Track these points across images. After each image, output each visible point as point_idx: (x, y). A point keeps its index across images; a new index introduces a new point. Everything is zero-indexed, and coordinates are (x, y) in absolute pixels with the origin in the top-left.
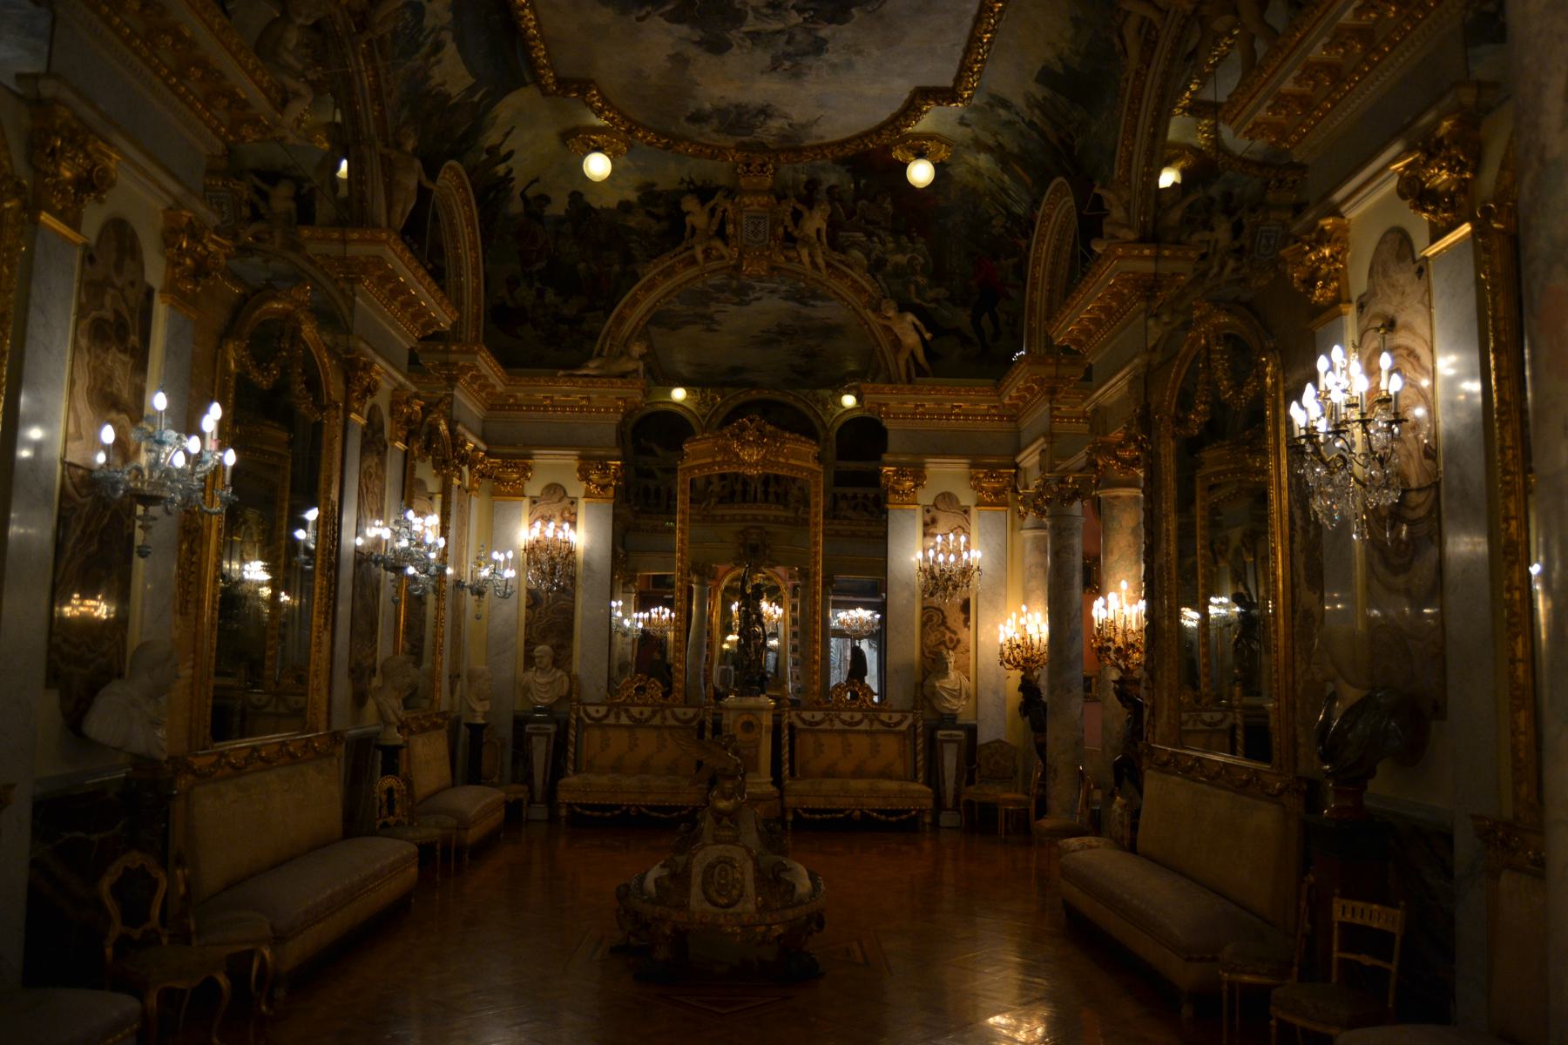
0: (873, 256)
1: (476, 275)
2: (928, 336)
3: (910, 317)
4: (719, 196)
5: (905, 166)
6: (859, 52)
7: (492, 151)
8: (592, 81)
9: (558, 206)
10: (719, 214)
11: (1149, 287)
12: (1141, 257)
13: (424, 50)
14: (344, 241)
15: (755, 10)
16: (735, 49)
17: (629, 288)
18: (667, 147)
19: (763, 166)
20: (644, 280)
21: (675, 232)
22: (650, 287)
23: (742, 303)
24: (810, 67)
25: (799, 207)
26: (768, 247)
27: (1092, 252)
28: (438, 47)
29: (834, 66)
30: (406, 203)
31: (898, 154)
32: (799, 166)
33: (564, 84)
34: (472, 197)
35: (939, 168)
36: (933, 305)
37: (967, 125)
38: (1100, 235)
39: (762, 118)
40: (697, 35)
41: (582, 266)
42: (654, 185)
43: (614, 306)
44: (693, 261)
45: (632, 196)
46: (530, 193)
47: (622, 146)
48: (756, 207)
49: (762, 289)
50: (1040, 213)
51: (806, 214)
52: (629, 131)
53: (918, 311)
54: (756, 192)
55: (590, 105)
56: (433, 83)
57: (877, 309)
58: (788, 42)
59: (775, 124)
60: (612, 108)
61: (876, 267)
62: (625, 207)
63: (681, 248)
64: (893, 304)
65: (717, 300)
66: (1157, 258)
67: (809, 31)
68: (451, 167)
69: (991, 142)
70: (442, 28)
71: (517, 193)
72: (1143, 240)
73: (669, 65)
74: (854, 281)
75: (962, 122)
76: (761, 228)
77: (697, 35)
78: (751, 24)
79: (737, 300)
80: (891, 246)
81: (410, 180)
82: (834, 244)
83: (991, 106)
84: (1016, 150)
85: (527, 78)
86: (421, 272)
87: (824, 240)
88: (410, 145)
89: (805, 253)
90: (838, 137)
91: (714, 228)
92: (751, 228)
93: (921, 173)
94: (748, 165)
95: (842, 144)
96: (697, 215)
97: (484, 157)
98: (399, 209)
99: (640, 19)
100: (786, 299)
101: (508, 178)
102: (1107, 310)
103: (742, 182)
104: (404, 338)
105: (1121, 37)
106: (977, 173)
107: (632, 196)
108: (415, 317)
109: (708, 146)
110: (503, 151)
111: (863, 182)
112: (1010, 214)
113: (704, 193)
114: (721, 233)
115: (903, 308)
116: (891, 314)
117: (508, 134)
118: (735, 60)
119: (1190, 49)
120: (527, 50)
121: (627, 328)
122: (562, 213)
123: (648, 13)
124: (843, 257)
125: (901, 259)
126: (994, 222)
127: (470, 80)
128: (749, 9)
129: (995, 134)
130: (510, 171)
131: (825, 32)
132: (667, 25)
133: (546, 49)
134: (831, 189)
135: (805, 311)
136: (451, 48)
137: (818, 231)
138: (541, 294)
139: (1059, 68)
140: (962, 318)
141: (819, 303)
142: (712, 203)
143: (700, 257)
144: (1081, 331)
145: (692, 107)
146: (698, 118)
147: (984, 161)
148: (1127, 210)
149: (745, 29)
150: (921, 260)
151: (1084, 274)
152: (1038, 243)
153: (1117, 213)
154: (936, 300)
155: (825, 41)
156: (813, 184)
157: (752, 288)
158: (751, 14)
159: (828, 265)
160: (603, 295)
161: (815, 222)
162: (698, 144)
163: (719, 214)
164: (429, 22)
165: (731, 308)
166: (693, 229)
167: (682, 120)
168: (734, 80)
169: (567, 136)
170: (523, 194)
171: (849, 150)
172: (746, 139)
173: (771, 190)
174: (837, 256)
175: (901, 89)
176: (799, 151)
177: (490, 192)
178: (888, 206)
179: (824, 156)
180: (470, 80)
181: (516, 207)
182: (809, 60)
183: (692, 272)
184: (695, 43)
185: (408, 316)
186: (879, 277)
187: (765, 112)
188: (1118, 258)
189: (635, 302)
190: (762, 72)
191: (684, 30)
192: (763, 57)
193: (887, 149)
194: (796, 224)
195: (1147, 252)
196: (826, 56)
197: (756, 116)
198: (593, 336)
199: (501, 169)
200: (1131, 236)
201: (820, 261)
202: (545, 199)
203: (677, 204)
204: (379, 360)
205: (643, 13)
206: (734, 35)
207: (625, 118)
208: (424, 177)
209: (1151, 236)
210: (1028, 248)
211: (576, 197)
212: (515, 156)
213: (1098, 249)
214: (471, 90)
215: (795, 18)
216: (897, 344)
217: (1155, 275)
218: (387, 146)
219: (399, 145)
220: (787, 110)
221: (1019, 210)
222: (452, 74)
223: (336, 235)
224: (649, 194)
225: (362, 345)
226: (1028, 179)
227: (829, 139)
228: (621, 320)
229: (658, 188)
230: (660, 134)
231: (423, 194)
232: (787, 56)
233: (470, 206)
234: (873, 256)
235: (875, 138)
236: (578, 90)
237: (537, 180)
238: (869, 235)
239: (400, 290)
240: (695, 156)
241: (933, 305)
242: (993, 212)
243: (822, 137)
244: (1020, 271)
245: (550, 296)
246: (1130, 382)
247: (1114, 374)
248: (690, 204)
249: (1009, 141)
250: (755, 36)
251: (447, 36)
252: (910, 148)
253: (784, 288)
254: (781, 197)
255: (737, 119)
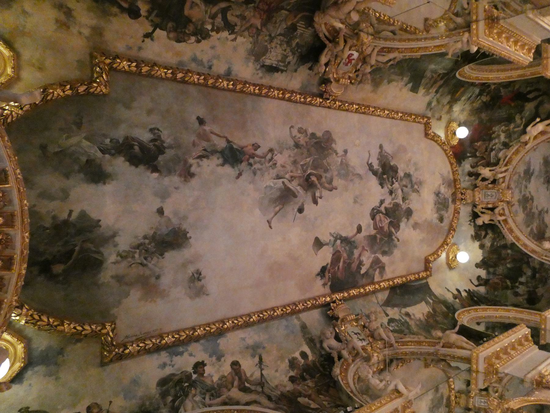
0: (502, 147)
1: (509, 311)
2: (538, 120)
3: (529, 128)
4: (476, 210)
5: (460, 140)
6: (410, 161)
7: (455, 297)
8: (425, 258)
9: (483, 273)
10: (484, 210)
11: (492, 21)
12: (477, 29)
13: (408, 319)
14: (477, 372)
15: (393, 199)
16: (411, 206)
17: (518, 247)
18: (454, 230)
19: (462, 194)
20: (514, 241)
21: (491, 227)
22: (518, 239)
23: (532, 199)
24: (417, 178)
25: (480, 178)
26: (498, 190)
27: (478, 51)
28: (407, 314)
29: (416, 170)
30: (462, 340)
31: (455, 142)
32: (462, 180)
33: (427, 268)
34: (473, 308)
35: (460, 125)
36: (524, 120)
37: (441, 117)
38: (469, 51)
39: (440, 195)
40: (404, 220)
41: (509, 266)
42: (472, 236)
43: (526, 254)
44: (505, 221)
45: (477, 244)
46: (476, 283)
47: (455, 247)
48: (480, 196)
49: (525, 191)
50: (477, 82)
51: (483, 176)
52: (447, 245)
53: (526, 125)
54: (474, 196)
55: (435, 259)
56: (422, 318)
57: (526, 143)
58: (406, 187)
59: (443, 190)
60: (437, 251)
61: (506, 146)
62: (482, 247)
63: (499, 225)
64: (523, 136)
65: (531, 209)
66: (477, 21)
67: (401, 180)
68: (459, 315)
69: (448, 107)
70: (400, 312)
71: (476, 289)
72: (469, 31)
73: (418, 230)
74: (513, 153)
75: (440, 119)
76: (489, 193)
77: (404, 220)
78: (399, 201)
79: (531, 202)
80: (497, 141)
81: (453, 337)
82: (496, 164)
83: (431, 109)
84: (450, 96)
85: (424, 281)
86: (496, 339)
87: (494, 168)
88: (439, 334)
89: (500, 176)
90: (449, 166)
91: (490, 212)
92: (489, 197)
93: (463, 133)
94: (462, 199)
95: (451, 164)
96: (485, 219)
97: (457, 300)
98: (465, 345)
99: (398, 240)
100: (530, 182)
101: (469, 292)
102: (508, 39)
103: (469, 201)
104: (535, 351)
105: (390, 60)
106: (463, 110)
107: (477, 244)
108: (521, 344)
109: (454, 215)
110: (456, 292)
111: (468, 155)
112: (480, 94)
113: (475, 216)
114: (492, 209)
115: (524, 132)
116: (527, 138)
117: (448, 290)
118: (414, 205)
119: (391, 34)
120: (411, 281)
121: (537, 249)
122: (485, 271)
123: (396, 237)
124: (502, 160)
125: (503, 137)
126: (485, 100)
127: (423, 303)
128: (393, 202)
129: (443, 106)
130: (465, 290)
131: (401, 174)
132: (400, 231)
133: (411, 274)
134: (472, 167)
135: (536, 173)
136: (409, 310)
137: (490, 171)
138: (521, 283)
139: (410, 85)
140: (530, 107)
141: (532, 168)
142: (480, 214)
143: (503, 218)
144: (523, 49)
145: (436, 221)
146: (441, 219)
147: (457, 108)
148: (458, 41)
149: (401, 203)
150: (503, 127)
151: (493, 54)
152: (489, 80)
153: (459, 45)
154: (521, 119)
155: (405, 174)
156: (470, 174)
157: (524, 196)
158: (395, 201)
159: (506, 165)
160: (522, 258)
161: (486, 172)
162: (453, 219)
163: (484, 210)
164: (397, 317)
165: (535, 203)
166: (491, 220)
167: (442, 225)
168: (424, 206)
169: (450, 268)
170: (476, 286)
171: (453, 161)
172: (450, 200)
173: (473, 190)
174: (501, 162)
175: (426, 143)
176: (455, 181)
177: (473, 299)
178: (479, 144)
179: (456, 170)
180: (423, 303)
181: (482, 290)
182: (414, 179)
183: (510, 221)
184: (408, 220)
185: (519, 348)
186: (511, 144)
187: (438, 194)
188: (478, 38)
189: (525, 245)
190: (420, 196)
191: (402, 225)
192: (413, 196)
193: (453, 147)
194: (487, 180)
195: (474, 27)
196: (412, 173)
197: (439, 197)
198: (542, 264)
199: (464, 294)
200: (467, 35)
201: (504, 169)
202: (479, 278)
203: (480, 227)
204: (540, 368)
205: (396, 239)
206: (404, 206)
207: (442, 246)
208: (453, 331)
209: (468, 27)
210: (495, 84)
211: (477, 266)
212: (458, 288)
213: (475, 49)
214: (427, 303)
215: (396, 185)
216: (542, 133)
217: (485, 19)
218: (440, 343)
219: (440, 338)
220: (436, 185)
221: (477, 91)
222: (420, 311)
223: (474, 374)
224: (477, 237)
225: (530, 376)
226: (462, 89)
227: (450, 170)
228: (533, 251)
229: (473, 234)
230: (449, 232)
231: (465, 332)
232: (412, 187)
233: (477, 309)
234: (502, 147)
235: (447, 152)
236: (429, 263)
237: (471, 280)
238: (492, 150)
239: (505, 351)
240: (458, 219)
241: (524, 120)
242: (480, 101)
243: (449, 172)
244: (508, 85)
245: (523, 279)
246: (544, 16)
247: (542, 26)
248: (479, 222)
249: (446, 99)
250: (404, 199)
251: (404, 310)
252: (452, 138)
253: (524, 183)
254: (475, 186)
255: (441, 205)
